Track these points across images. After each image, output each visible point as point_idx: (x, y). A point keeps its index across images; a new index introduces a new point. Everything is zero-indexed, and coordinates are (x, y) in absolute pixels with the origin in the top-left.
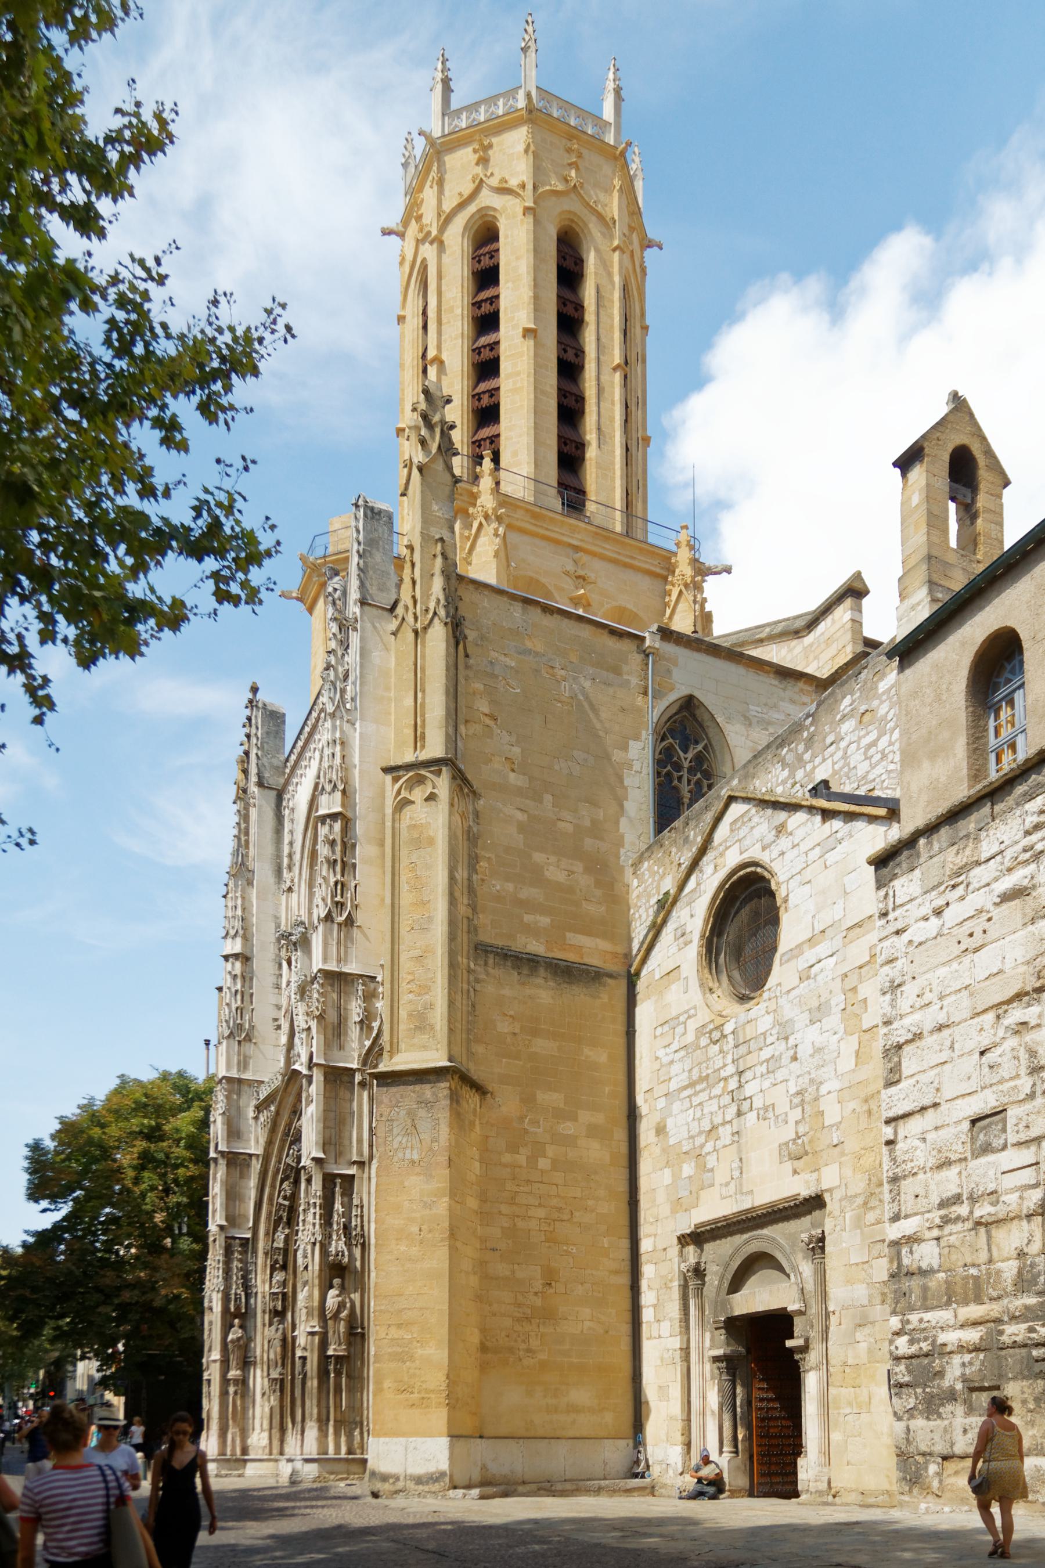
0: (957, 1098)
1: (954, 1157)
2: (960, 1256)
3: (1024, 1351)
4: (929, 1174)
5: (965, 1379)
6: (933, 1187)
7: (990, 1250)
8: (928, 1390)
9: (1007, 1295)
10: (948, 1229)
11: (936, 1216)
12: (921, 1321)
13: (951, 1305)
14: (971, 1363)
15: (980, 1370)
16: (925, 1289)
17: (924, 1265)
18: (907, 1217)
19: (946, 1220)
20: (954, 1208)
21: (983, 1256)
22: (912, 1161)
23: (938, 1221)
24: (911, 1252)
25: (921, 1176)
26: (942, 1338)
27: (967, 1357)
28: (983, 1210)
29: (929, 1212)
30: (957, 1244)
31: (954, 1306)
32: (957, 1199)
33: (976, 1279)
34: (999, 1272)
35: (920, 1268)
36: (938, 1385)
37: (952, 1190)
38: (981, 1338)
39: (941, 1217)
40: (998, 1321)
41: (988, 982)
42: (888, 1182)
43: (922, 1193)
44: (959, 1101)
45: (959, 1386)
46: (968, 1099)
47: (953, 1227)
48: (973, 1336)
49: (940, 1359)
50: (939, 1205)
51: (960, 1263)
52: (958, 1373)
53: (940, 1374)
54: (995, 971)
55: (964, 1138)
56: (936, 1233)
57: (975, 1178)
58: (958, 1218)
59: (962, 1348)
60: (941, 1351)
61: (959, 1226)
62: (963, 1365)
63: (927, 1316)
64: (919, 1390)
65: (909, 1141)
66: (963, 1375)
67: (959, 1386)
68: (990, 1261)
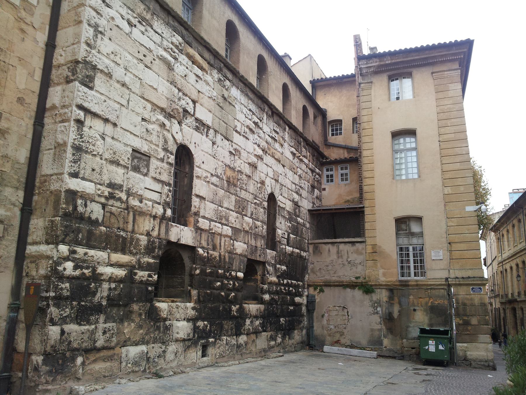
0: (128, 131)
1: (122, 162)
2: (116, 221)
3: (143, 286)
4: (104, 162)
5: (109, 298)
6: (105, 170)
7: (134, 225)
8: (83, 303)
9: (141, 253)
10: (111, 202)
11: (107, 191)
12: (86, 254)
13: (106, 250)
14: (115, 289)
15: (119, 294)
16: (90, 233)
17: (94, 217)
18: (83, 179)
19: (111, 196)
20: (117, 192)
21: (130, 227)
22: (94, 145)
23: (106, 194)
24: (86, 205)
25: (98, 159)
26: (101, 269)
27: (113, 285)
28: (134, 202)
29: (100, 185)
30: (116, 213)
31: (109, 251)
32: (120, 187)
33: (124, 239)
34: (138, 240)
35: (90, 218)
36: (91, 300)
37: (118, 180)
38: (125, 275)
39: (109, 193)
40: (133, 267)
41: (149, 87)
42: (72, 147)
43: (98, 170)
44: (129, 134)
45: (104, 303)
46: (132, 136)
47: (115, 202)
48: (121, 273)
49: (95, 283)
50: (108, 184)
51: (116, 226)
52: (105, 294)
53: (94, 294)
54: (155, 87)
55: (129, 156)
56: (103, 200)
57: (131, 181)
58: (120, 199)
59: (111, 279)
60: (96, 278)
61: (118, 204)
62: (110, 289)
63: (92, 252)
64: (74, 303)
65: (92, 130)
66: (108, 296)
67: (104, 303)
68: (133, 231)
